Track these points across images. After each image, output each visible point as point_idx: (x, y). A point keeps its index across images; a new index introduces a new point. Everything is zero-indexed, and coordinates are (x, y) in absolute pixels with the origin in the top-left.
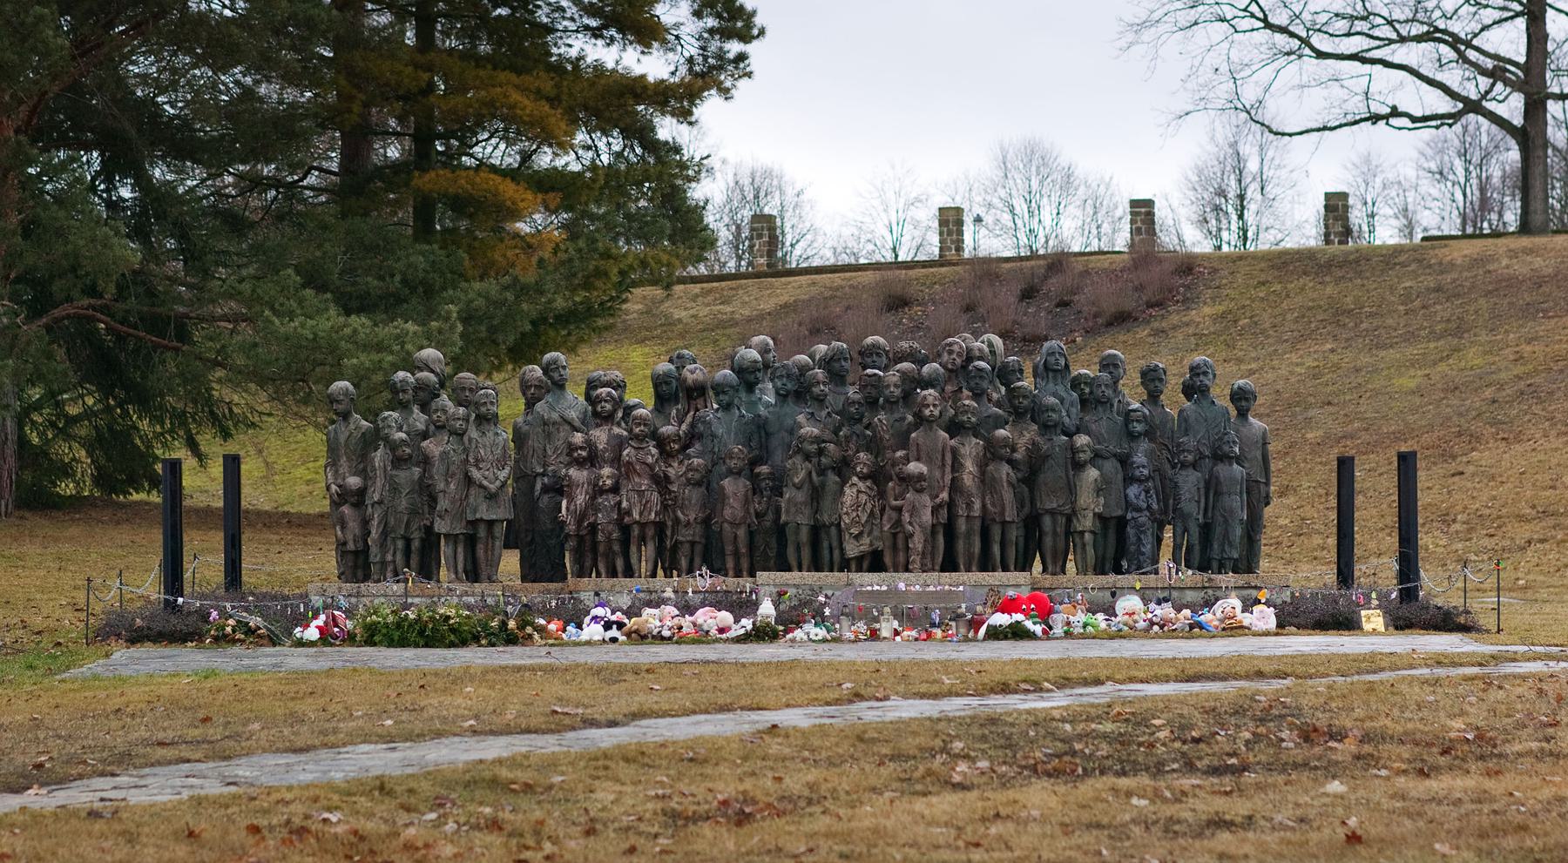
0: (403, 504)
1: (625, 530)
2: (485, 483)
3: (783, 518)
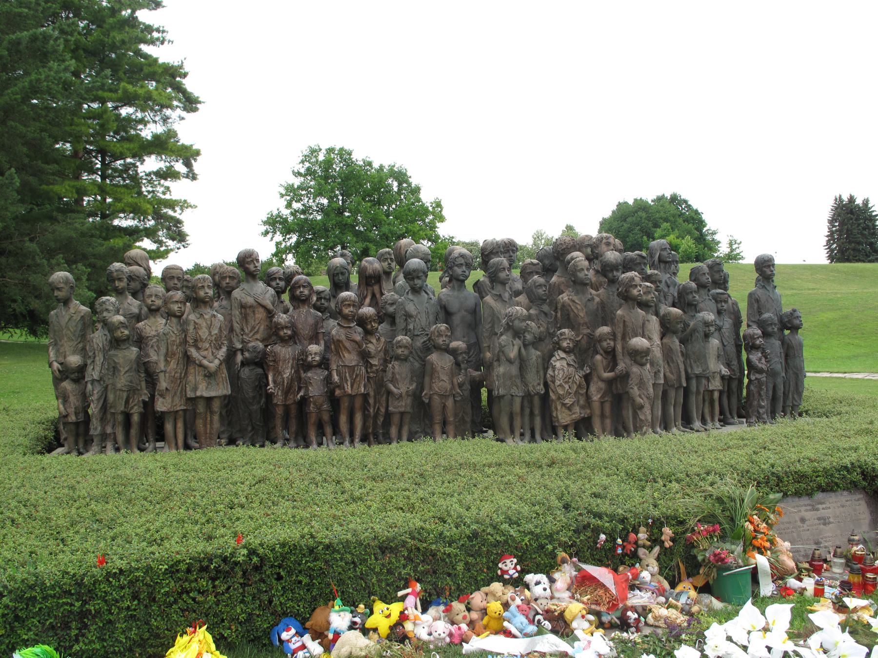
0: (122, 381)
1: (334, 402)
2: (205, 362)
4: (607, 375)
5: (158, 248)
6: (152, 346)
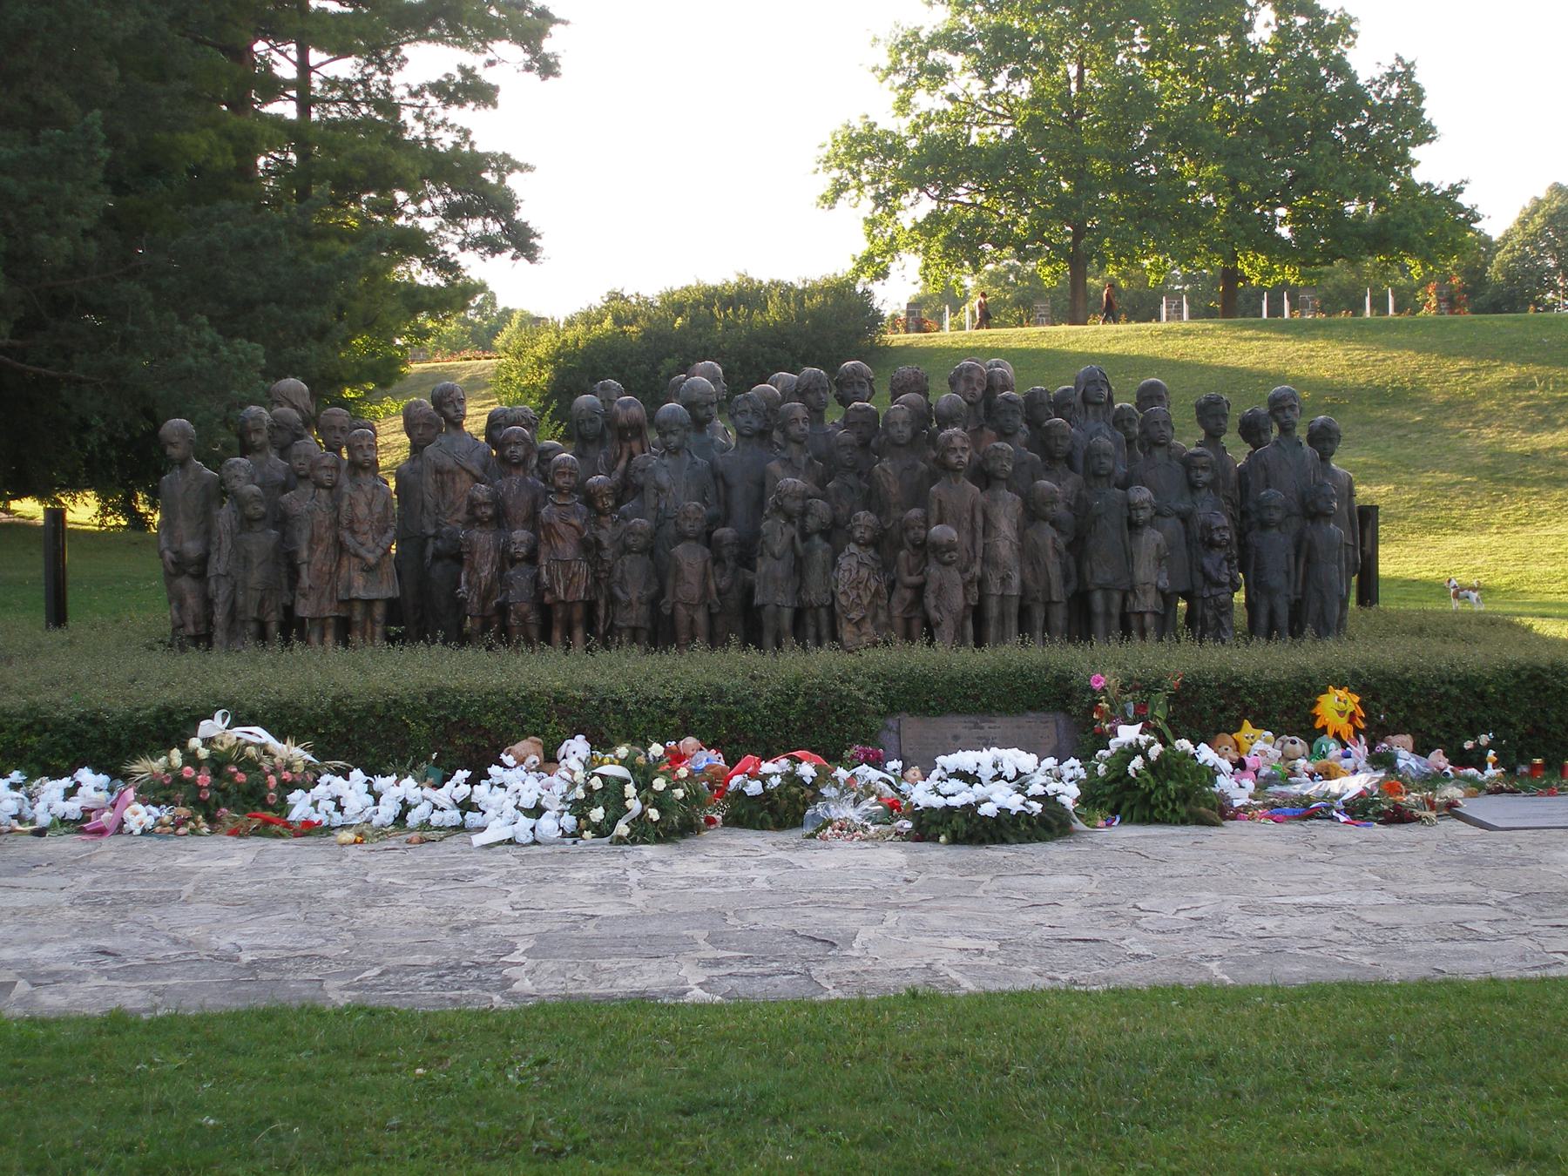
0: (256, 577)
2: (362, 552)
3: (758, 600)
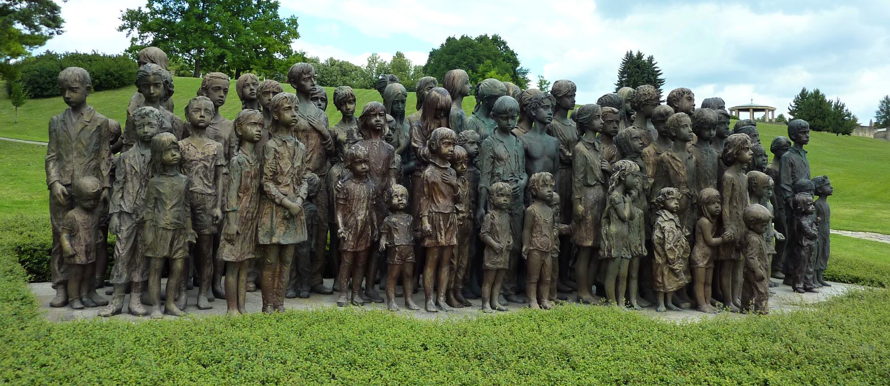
0: (167, 216)
2: (287, 202)
4: (716, 240)
5: (33, 33)
6: (197, 173)
